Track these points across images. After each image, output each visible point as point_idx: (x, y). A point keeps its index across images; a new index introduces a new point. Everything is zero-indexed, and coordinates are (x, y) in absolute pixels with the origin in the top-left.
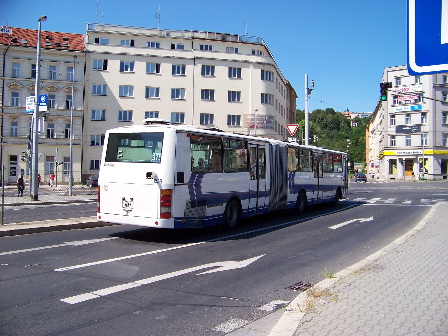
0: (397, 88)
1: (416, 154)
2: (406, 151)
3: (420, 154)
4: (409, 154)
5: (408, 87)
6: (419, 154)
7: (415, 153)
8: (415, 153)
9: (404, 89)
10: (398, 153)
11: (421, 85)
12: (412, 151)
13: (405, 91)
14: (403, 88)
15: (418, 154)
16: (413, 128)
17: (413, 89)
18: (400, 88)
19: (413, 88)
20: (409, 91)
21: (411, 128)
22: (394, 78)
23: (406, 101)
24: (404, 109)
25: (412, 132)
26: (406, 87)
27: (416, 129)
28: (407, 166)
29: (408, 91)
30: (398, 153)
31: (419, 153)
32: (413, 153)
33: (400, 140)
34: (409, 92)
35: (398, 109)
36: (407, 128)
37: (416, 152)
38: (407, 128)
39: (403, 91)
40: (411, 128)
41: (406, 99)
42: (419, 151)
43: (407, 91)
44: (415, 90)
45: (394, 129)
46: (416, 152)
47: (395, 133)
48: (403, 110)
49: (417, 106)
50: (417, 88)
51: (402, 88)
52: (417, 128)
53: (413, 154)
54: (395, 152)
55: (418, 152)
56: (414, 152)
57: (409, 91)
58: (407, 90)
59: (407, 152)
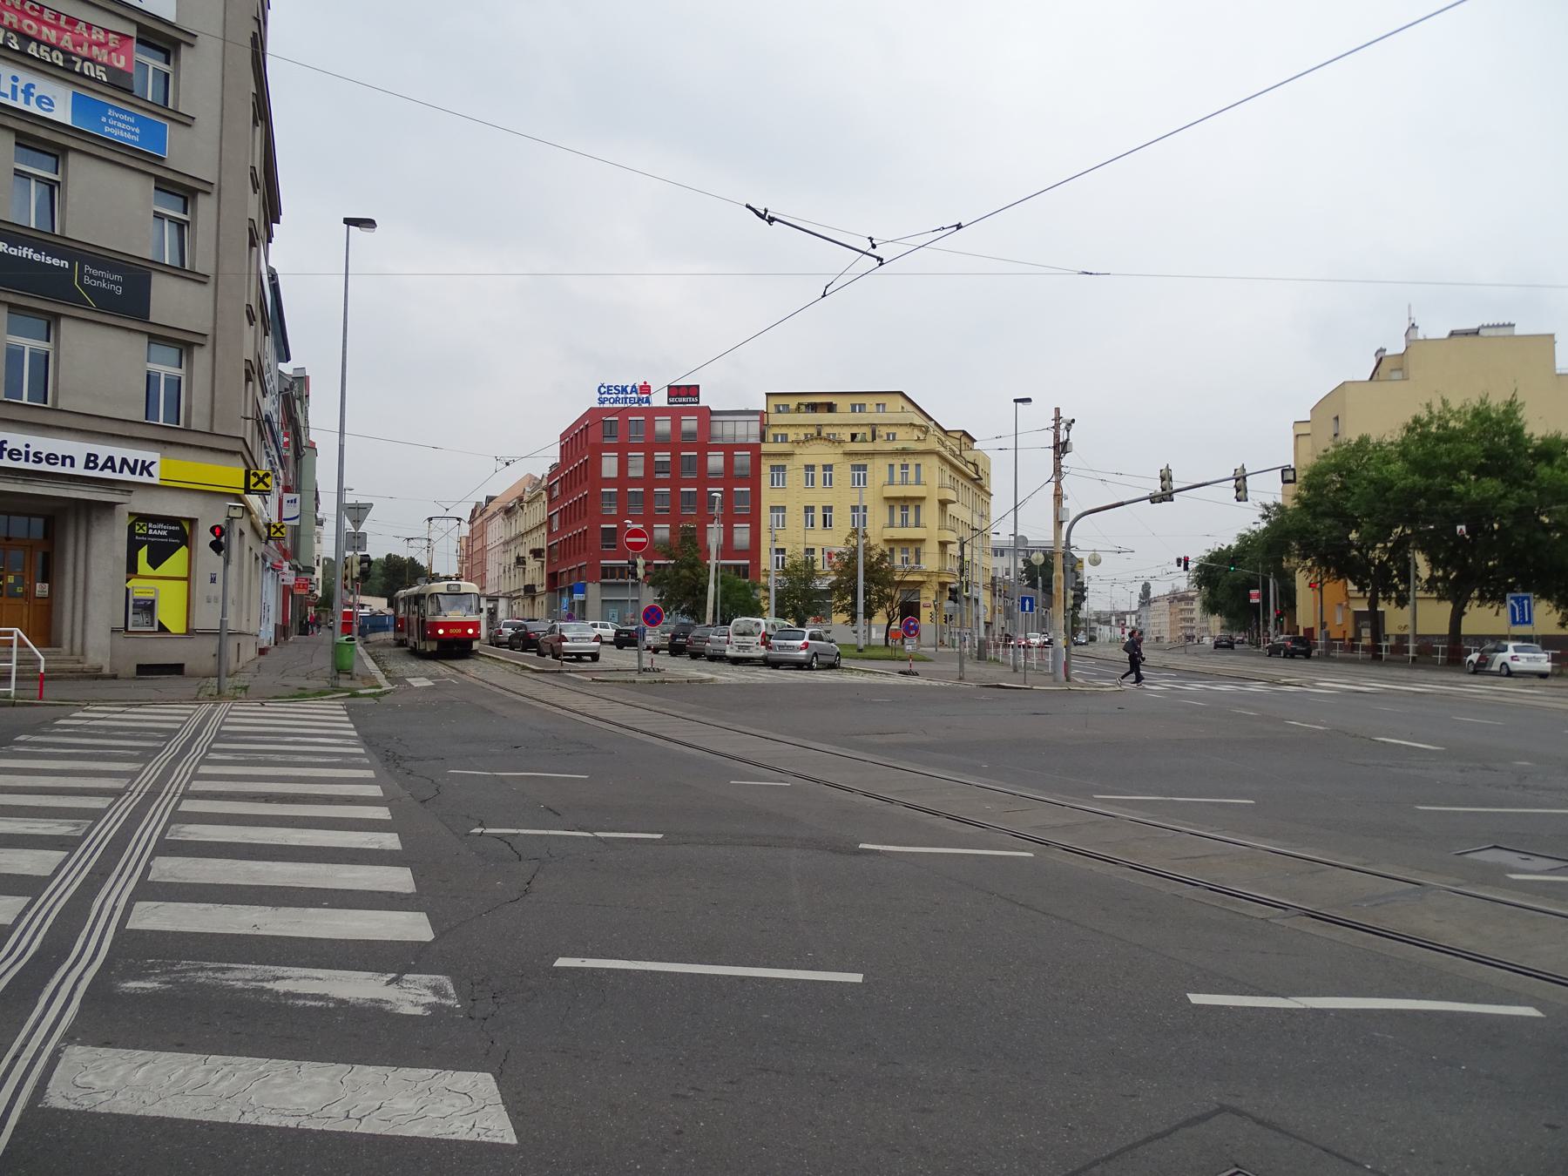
1: (107, 474)
3: (145, 479)
4: (44, 467)
6: (136, 478)
7: (101, 462)
8: (101, 462)
12: (78, 449)
15: (126, 476)
16: (87, 268)
21: (65, 264)
25: (79, 302)
27: (111, 282)
31: (133, 471)
32: (80, 461)
36: (26, 252)
37: (111, 459)
38: (26, 252)
40: (65, 264)
42: (133, 454)
46: (111, 459)
52: (119, 278)
53: (79, 470)
55: (124, 461)
56: (91, 460)
59: (23, 450)
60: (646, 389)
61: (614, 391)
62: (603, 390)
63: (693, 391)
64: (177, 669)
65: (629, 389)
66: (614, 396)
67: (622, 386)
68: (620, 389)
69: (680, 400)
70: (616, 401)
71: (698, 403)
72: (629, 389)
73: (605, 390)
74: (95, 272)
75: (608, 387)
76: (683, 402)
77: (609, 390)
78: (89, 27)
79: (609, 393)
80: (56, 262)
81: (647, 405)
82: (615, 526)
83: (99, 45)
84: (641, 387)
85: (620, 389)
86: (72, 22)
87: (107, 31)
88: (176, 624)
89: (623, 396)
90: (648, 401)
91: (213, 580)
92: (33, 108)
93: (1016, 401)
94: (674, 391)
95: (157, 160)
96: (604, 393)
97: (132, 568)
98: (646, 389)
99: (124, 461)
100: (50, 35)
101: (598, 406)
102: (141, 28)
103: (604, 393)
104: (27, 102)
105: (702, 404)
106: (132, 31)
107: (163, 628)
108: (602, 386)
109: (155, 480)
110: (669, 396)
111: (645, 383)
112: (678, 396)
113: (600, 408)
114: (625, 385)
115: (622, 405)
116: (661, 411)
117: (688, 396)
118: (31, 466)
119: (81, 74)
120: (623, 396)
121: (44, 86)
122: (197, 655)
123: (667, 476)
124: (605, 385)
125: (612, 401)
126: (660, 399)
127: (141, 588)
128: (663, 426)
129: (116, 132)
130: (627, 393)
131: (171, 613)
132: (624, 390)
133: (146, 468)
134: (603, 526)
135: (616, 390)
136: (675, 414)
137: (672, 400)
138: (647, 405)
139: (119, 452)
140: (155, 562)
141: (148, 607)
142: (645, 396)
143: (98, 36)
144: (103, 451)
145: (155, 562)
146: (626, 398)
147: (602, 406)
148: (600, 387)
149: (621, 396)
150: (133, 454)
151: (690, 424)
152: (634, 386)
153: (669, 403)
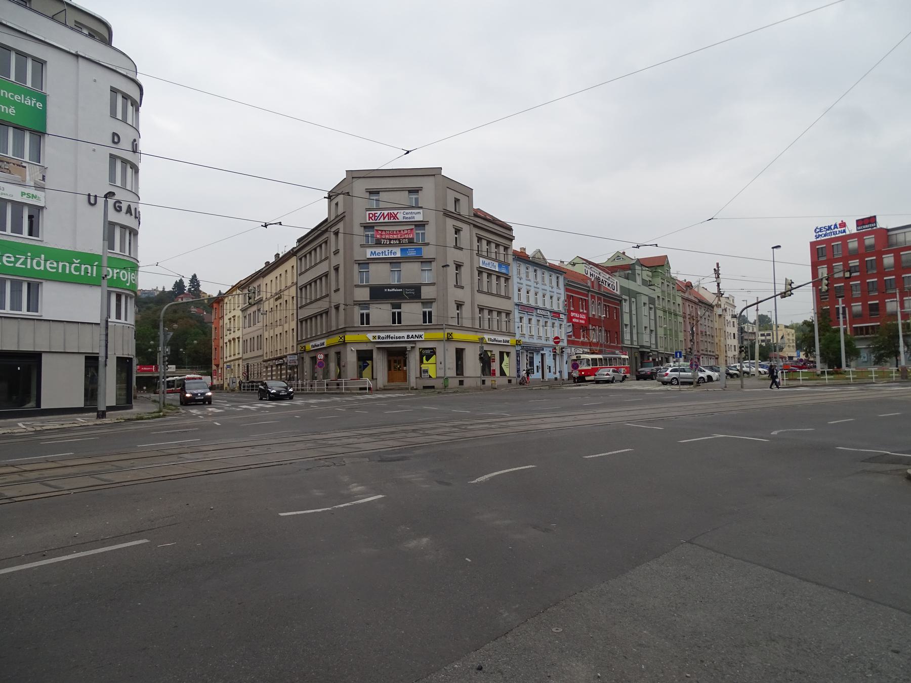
0: (373, 212)
1: (412, 339)
2: (392, 334)
3: (421, 339)
4: (398, 340)
5: (395, 212)
6: (419, 339)
7: (410, 337)
8: (410, 337)
9: (388, 214)
10: (374, 337)
11: (421, 211)
12: (405, 334)
13: (388, 219)
14: (386, 212)
15: (416, 339)
17: (406, 216)
18: (379, 212)
19: (404, 213)
20: (398, 219)
22: (364, 191)
23: (390, 240)
24: (387, 254)
26: (392, 212)
28: (392, 363)
29: (394, 219)
30: (374, 337)
31: (418, 338)
32: (406, 337)
33: (381, 313)
34: (397, 220)
35: (375, 252)
37: (412, 335)
39: (384, 219)
41: (391, 237)
42: (417, 333)
43: (392, 218)
44: (410, 218)
45: (367, 291)
46: (412, 335)
47: (369, 300)
48: (385, 255)
49: (413, 248)
50: (414, 215)
51: (383, 212)
52: (413, 290)
53: (406, 339)
54: (370, 336)
55: (416, 336)
56: (408, 336)
57: (398, 219)
58: (393, 216)
60: (843, 225)
61: (824, 230)
62: (818, 230)
63: (872, 220)
64: (433, 387)
65: (832, 227)
66: (824, 233)
67: (829, 226)
68: (827, 228)
69: (864, 227)
70: (825, 235)
71: (876, 226)
72: (832, 227)
73: (818, 230)
74: (408, 290)
75: (820, 228)
76: (867, 228)
77: (821, 230)
78: (403, 231)
79: (821, 232)
80: (399, 290)
81: (844, 234)
82: (877, 302)
83: (406, 234)
84: (840, 224)
85: (827, 228)
86: (400, 231)
87: (408, 230)
88: (434, 376)
89: (829, 231)
90: (844, 231)
91: (441, 363)
92: (393, 256)
93: (773, 248)
94: (860, 223)
95: (421, 257)
96: (818, 232)
97: (421, 362)
98: (843, 225)
99: (416, 336)
100: (395, 237)
101: (815, 240)
102: (416, 225)
103: (818, 232)
104: (391, 255)
105: (878, 227)
106: (413, 227)
107: (430, 377)
108: (817, 228)
109: (423, 339)
110: (858, 226)
111: (842, 221)
112: (863, 225)
113: (817, 241)
114: (830, 225)
115: (830, 237)
116: (852, 236)
117: (869, 223)
118: (395, 340)
119: (402, 243)
120: (829, 231)
121: (394, 249)
122: (439, 384)
123: (858, 274)
124: (819, 227)
125: (823, 236)
126: (852, 228)
127: (424, 367)
128: (853, 244)
129: (410, 254)
130: (831, 229)
131: (432, 373)
132: (830, 228)
133: (421, 336)
134: (869, 303)
135: (824, 228)
136: (859, 236)
137: (859, 228)
138: (844, 234)
139: (414, 334)
140: (427, 360)
141: (426, 371)
142: (843, 229)
143: (406, 232)
144: (410, 334)
145: (427, 360)
146: (831, 233)
147: (818, 239)
148: (816, 230)
149: (828, 232)
150: (414, 334)
151: (870, 240)
152: (835, 225)
153: (857, 230)
